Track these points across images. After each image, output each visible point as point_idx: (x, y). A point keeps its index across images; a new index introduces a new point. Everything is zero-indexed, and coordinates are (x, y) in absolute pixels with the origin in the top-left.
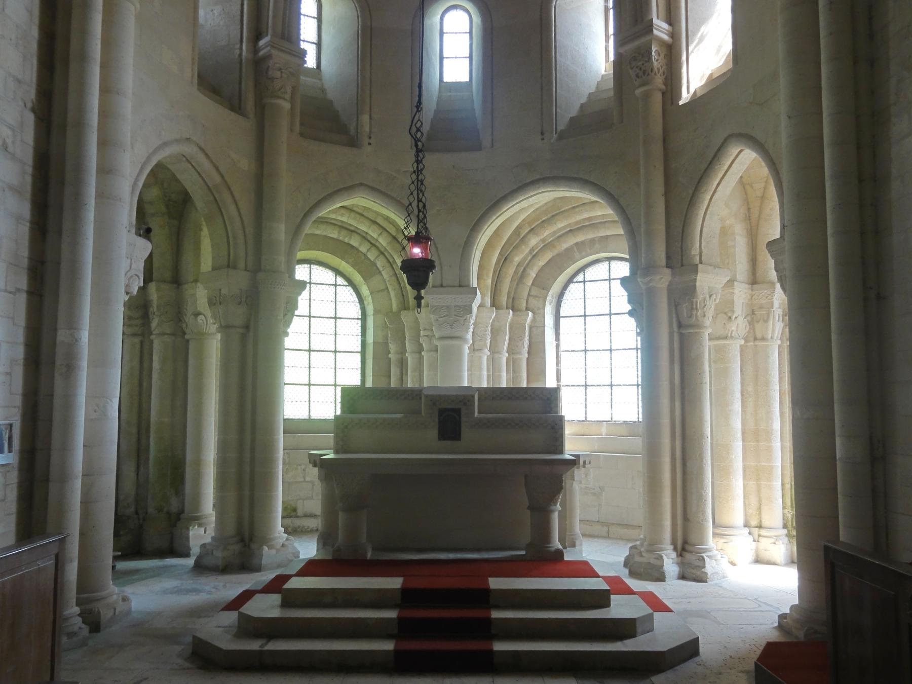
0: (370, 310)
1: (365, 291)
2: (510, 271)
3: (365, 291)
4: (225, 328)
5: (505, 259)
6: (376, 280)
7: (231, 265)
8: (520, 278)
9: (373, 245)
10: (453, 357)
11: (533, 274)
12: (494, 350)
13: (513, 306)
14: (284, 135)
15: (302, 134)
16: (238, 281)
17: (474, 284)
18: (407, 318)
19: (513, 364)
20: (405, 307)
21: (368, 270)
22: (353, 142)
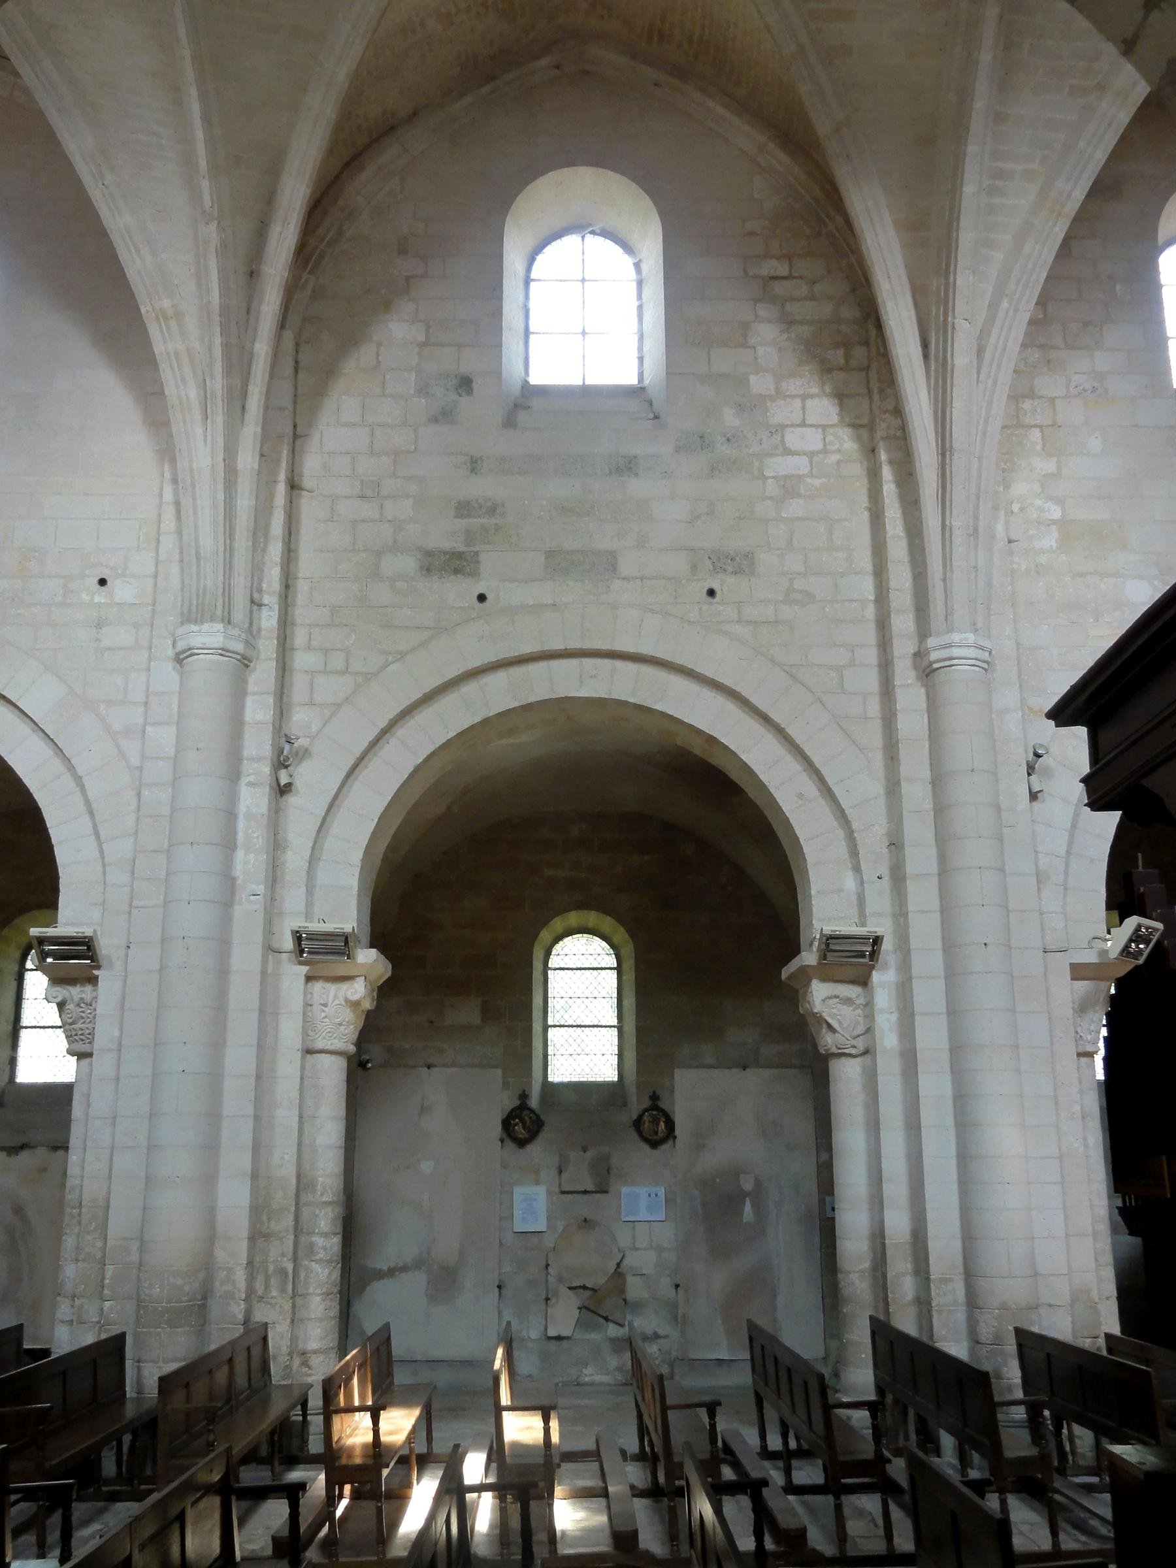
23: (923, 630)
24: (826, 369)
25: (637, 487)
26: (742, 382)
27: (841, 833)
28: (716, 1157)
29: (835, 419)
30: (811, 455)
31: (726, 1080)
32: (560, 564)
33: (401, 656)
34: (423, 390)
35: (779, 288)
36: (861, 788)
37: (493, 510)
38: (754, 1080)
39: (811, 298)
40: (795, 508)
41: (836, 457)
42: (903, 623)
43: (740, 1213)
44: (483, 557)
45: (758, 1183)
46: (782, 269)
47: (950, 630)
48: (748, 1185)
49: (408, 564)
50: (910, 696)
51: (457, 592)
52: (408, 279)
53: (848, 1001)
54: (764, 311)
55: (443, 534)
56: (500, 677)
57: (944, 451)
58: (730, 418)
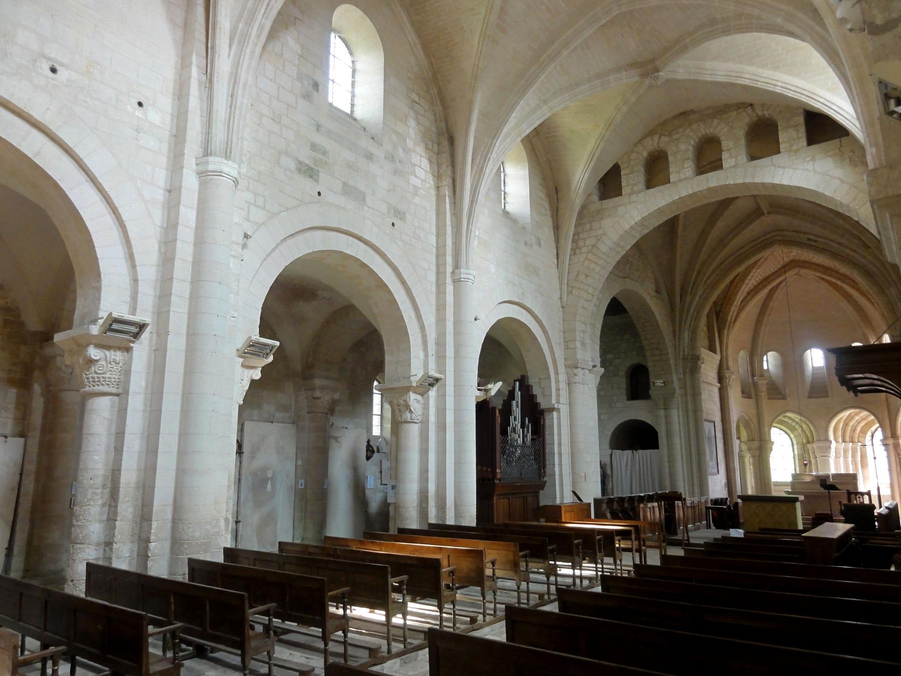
0: (795, 442)
1: (792, 436)
2: (849, 429)
3: (792, 436)
4: (753, 456)
5: (846, 424)
6: (796, 432)
7: (753, 440)
8: (854, 430)
9: (793, 420)
10: (827, 463)
11: (859, 429)
12: (846, 457)
13: (852, 441)
14: (764, 401)
15: (769, 399)
16: (756, 444)
17: (831, 437)
18: (809, 446)
19: (854, 462)
20: (809, 442)
21: (793, 429)
22: (784, 398)
23: (457, 266)
24: (427, 148)
25: (374, 168)
26: (405, 139)
27: (420, 335)
28: (258, 463)
29: (428, 170)
30: (422, 181)
31: (265, 427)
32: (349, 191)
33: (287, 209)
34: (300, 78)
35: (417, 107)
36: (430, 318)
37: (324, 153)
38: (276, 428)
39: (424, 116)
40: (417, 200)
41: (428, 185)
42: (449, 260)
43: (266, 487)
44: (321, 174)
45: (274, 473)
46: (417, 99)
47: (468, 268)
48: (270, 475)
49: (292, 165)
50: (450, 288)
51: (310, 187)
52: (295, 18)
53: (418, 401)
54: (412, 113)
55: (305, 155)
56: (319, 234)
57: (473, 202)
58: (400, 153)
